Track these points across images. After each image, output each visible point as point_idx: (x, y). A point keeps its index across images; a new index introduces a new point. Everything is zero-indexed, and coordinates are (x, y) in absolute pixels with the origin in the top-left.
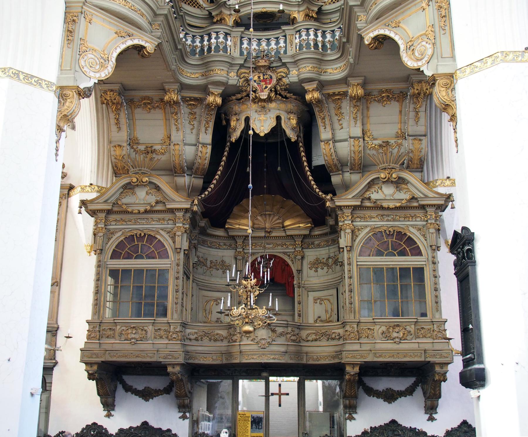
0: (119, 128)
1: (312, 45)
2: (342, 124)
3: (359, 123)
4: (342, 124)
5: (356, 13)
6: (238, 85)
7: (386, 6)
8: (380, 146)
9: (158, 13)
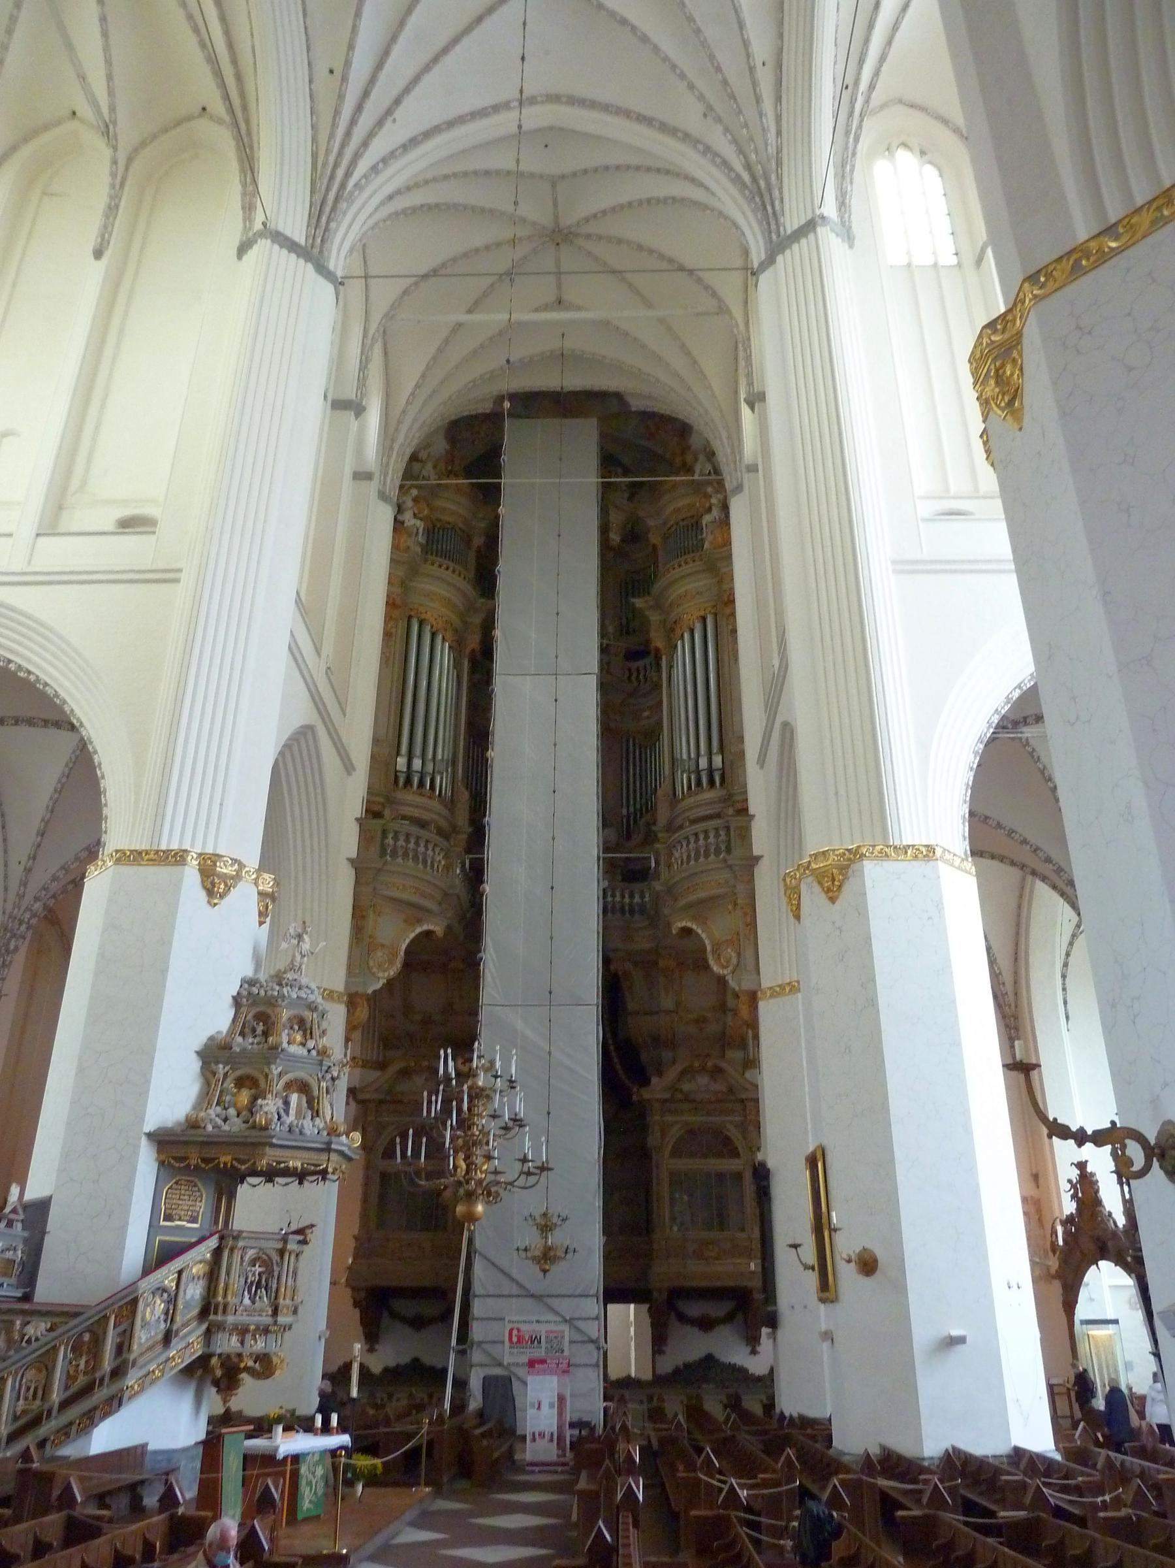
8: (697, 1021)
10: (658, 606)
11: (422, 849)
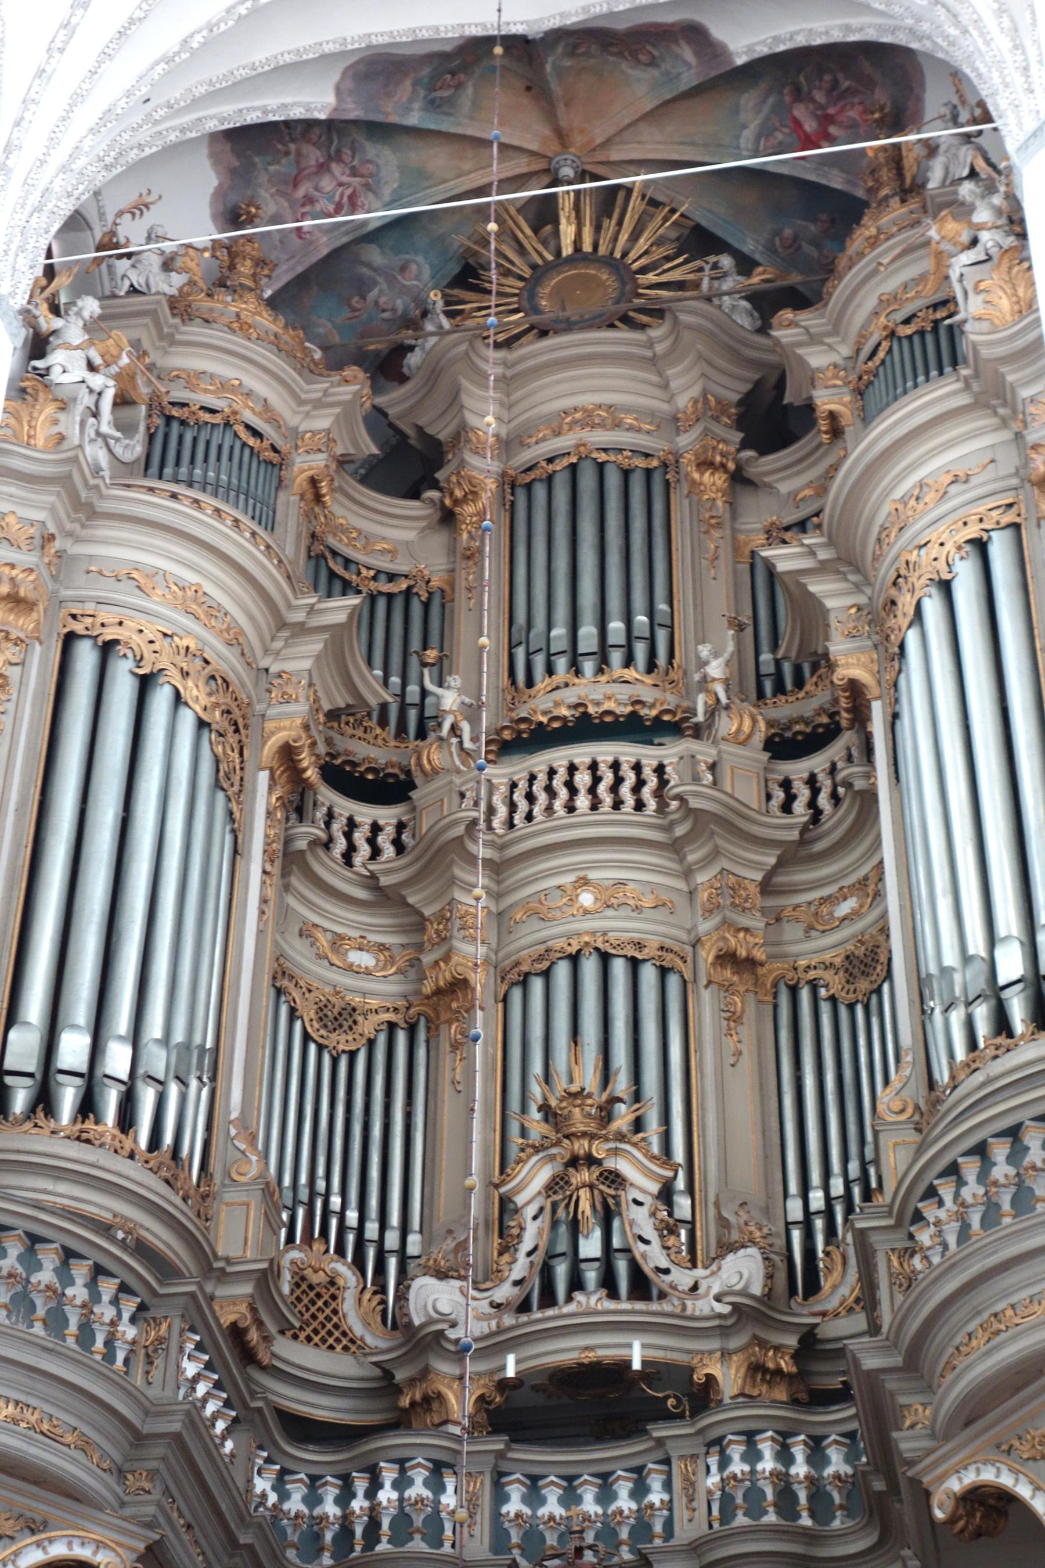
1: (770, 1496)
5: (892, 1394)
7: (988, 1381)
9: (146, 1429)
10: (848, 562)
11: (46, 1276)
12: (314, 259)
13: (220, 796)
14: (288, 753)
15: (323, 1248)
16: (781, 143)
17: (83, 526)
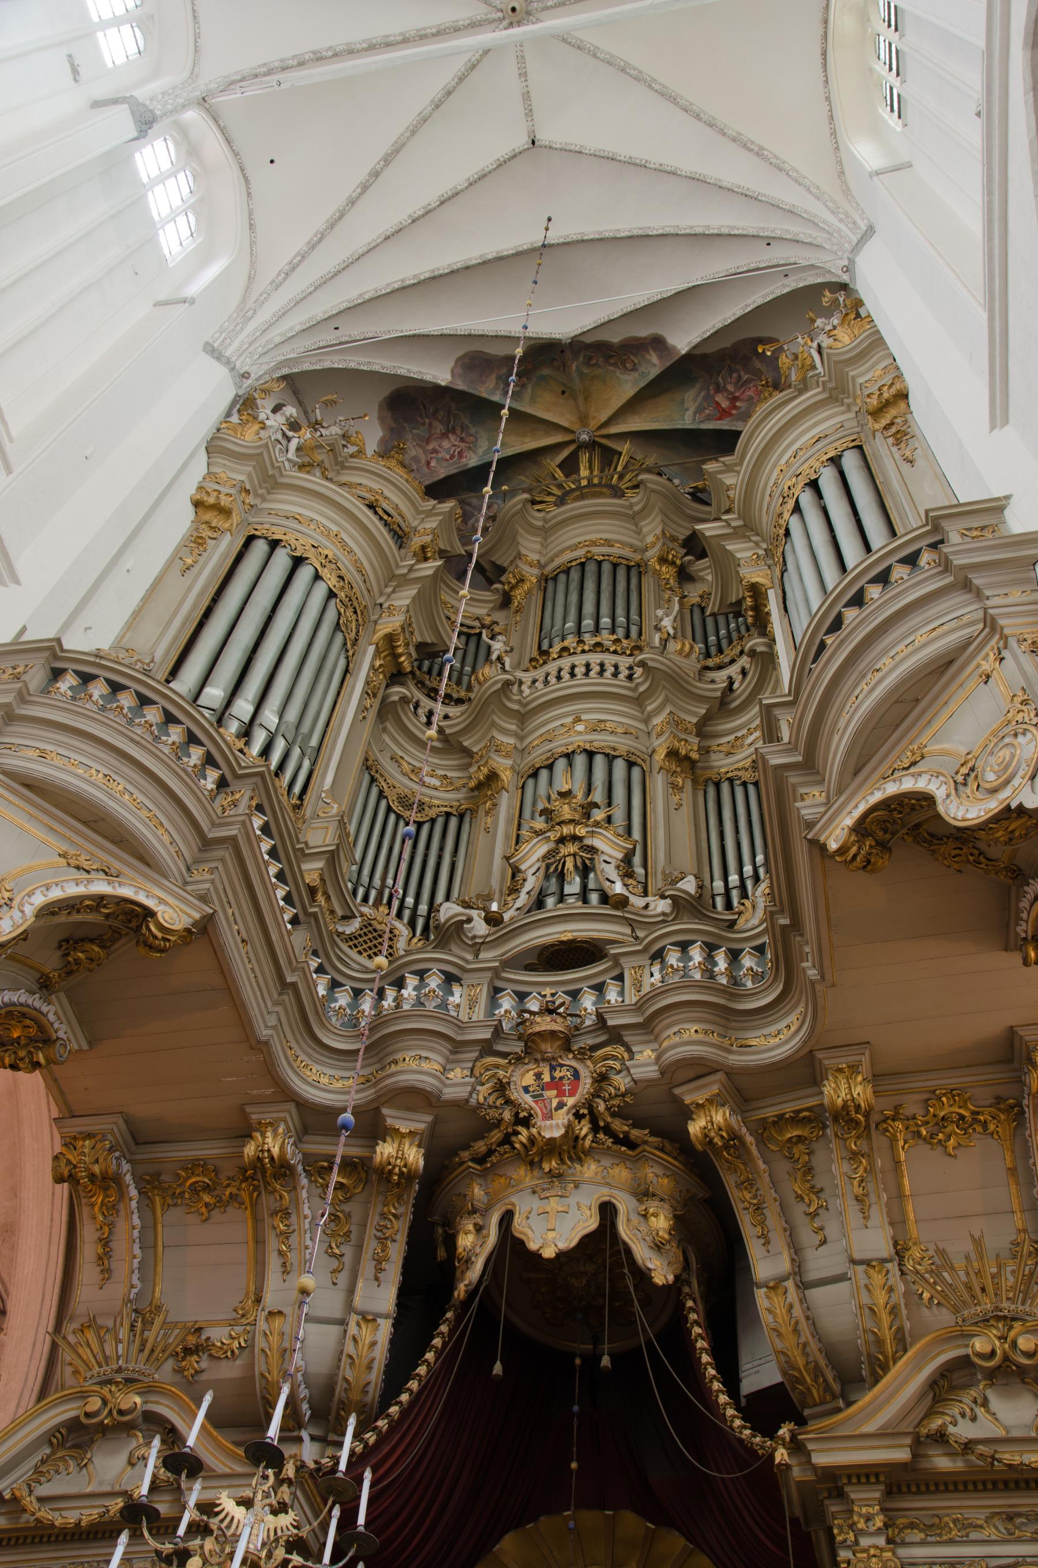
0: (107, 1273)
2: (821, 1229)
3: (878, 1215)
4: (821, 1229)
6: (473, 1101)
12: (436, 479)
13: (343, 656)
14: (390, 639)
15: (386, 911)
16: (708, 415)
17: (269, 493)
